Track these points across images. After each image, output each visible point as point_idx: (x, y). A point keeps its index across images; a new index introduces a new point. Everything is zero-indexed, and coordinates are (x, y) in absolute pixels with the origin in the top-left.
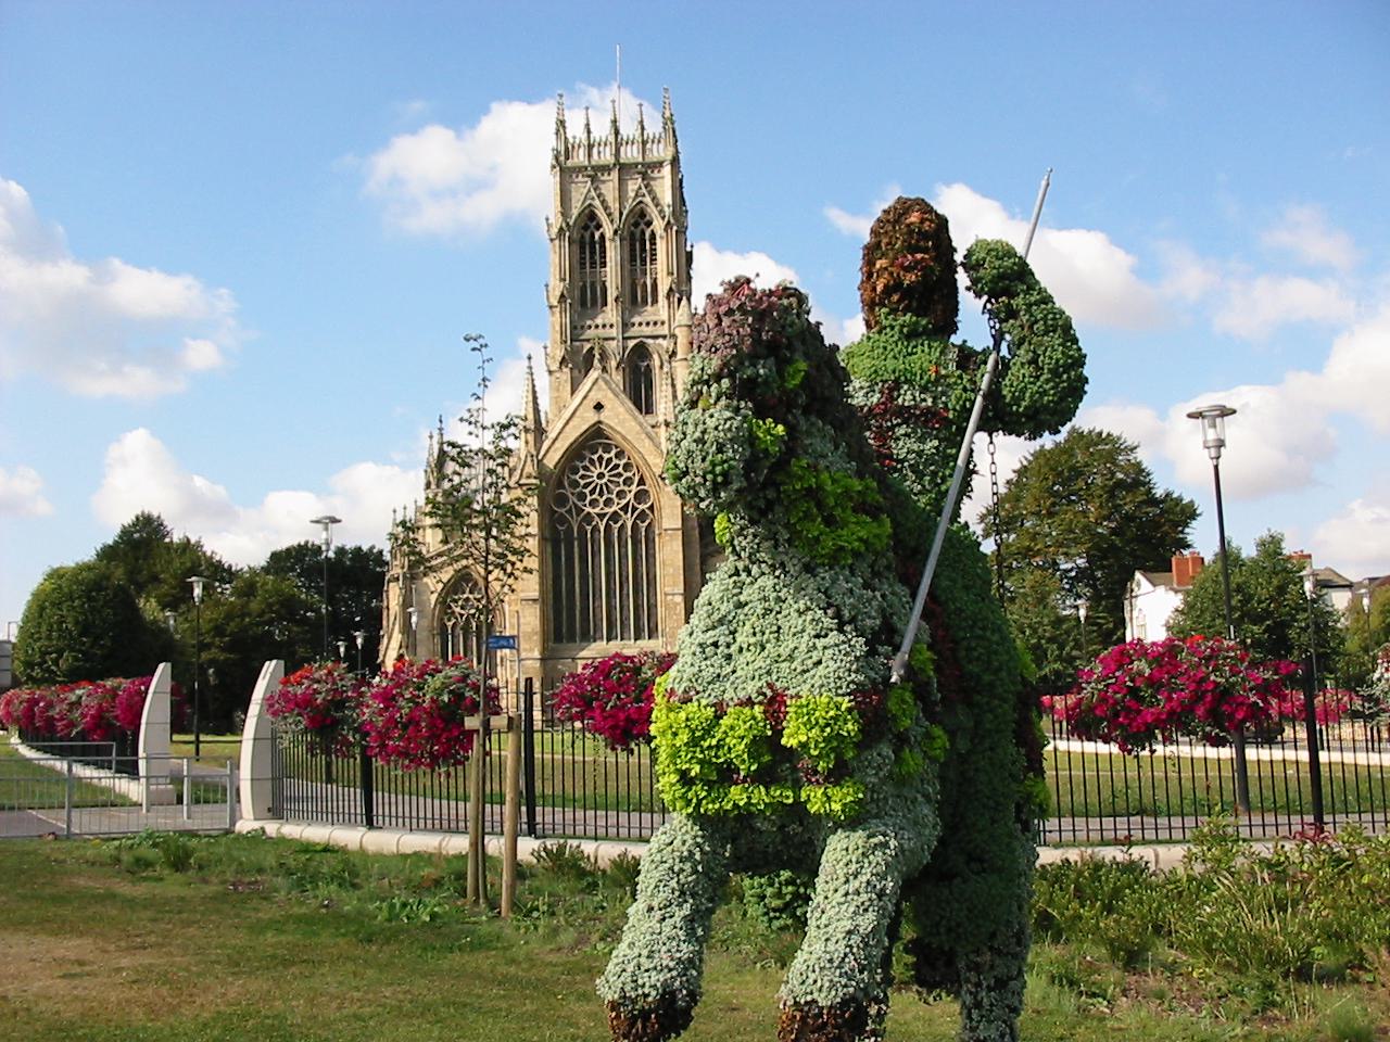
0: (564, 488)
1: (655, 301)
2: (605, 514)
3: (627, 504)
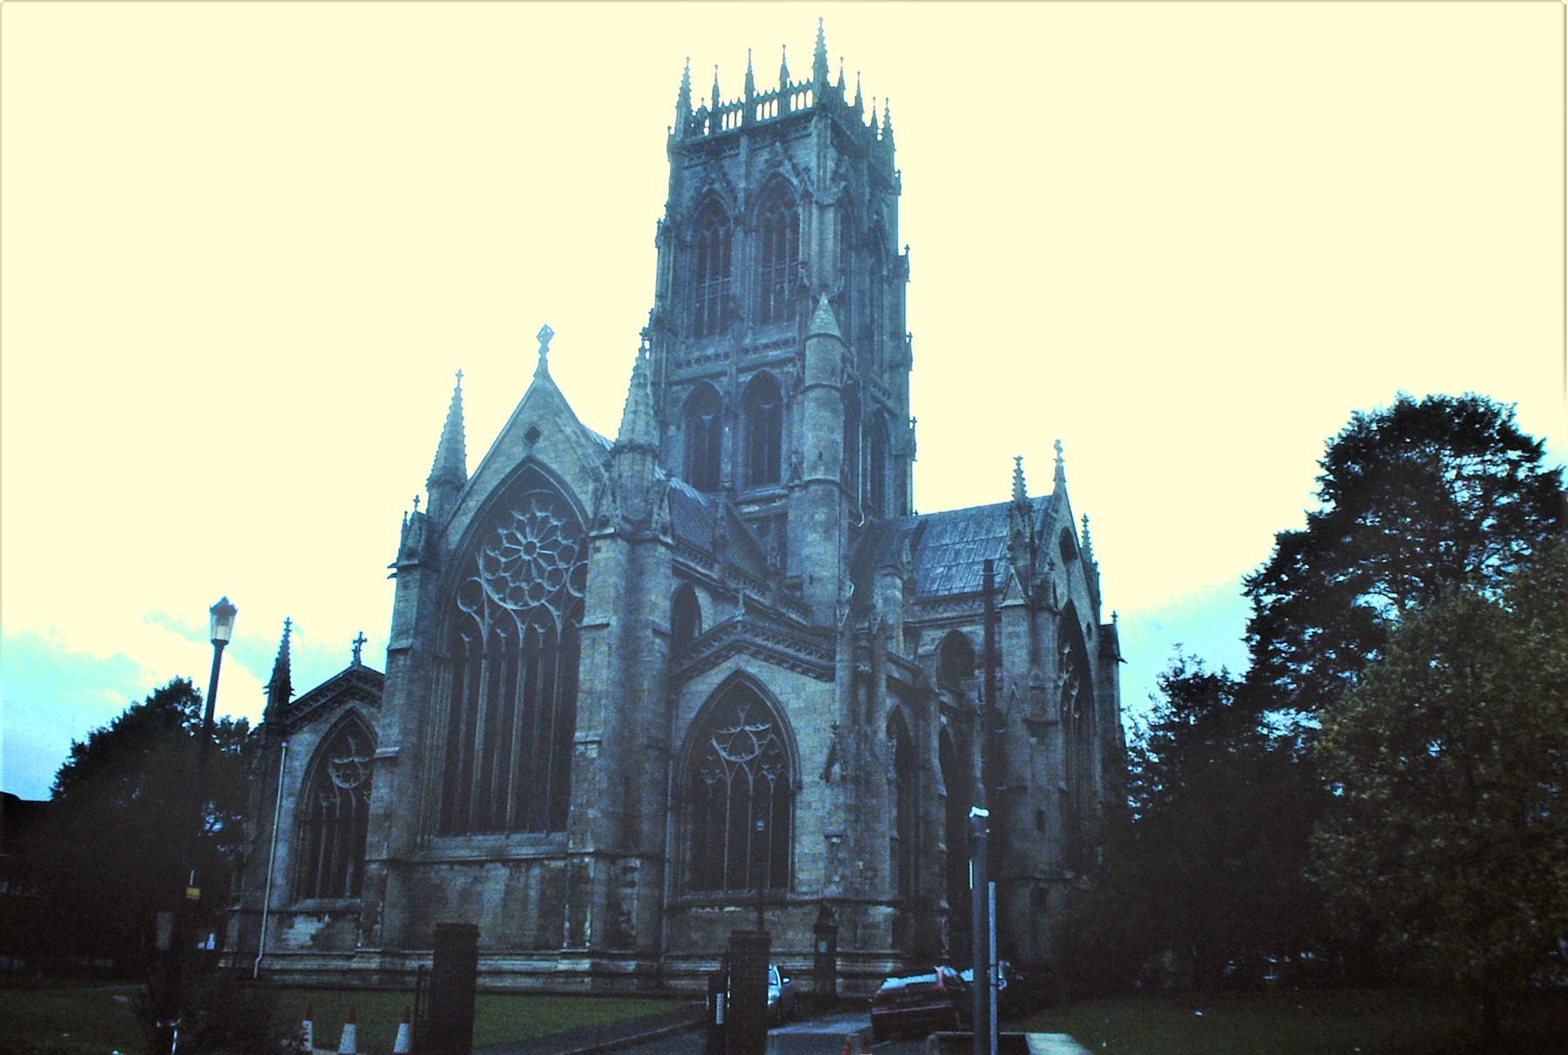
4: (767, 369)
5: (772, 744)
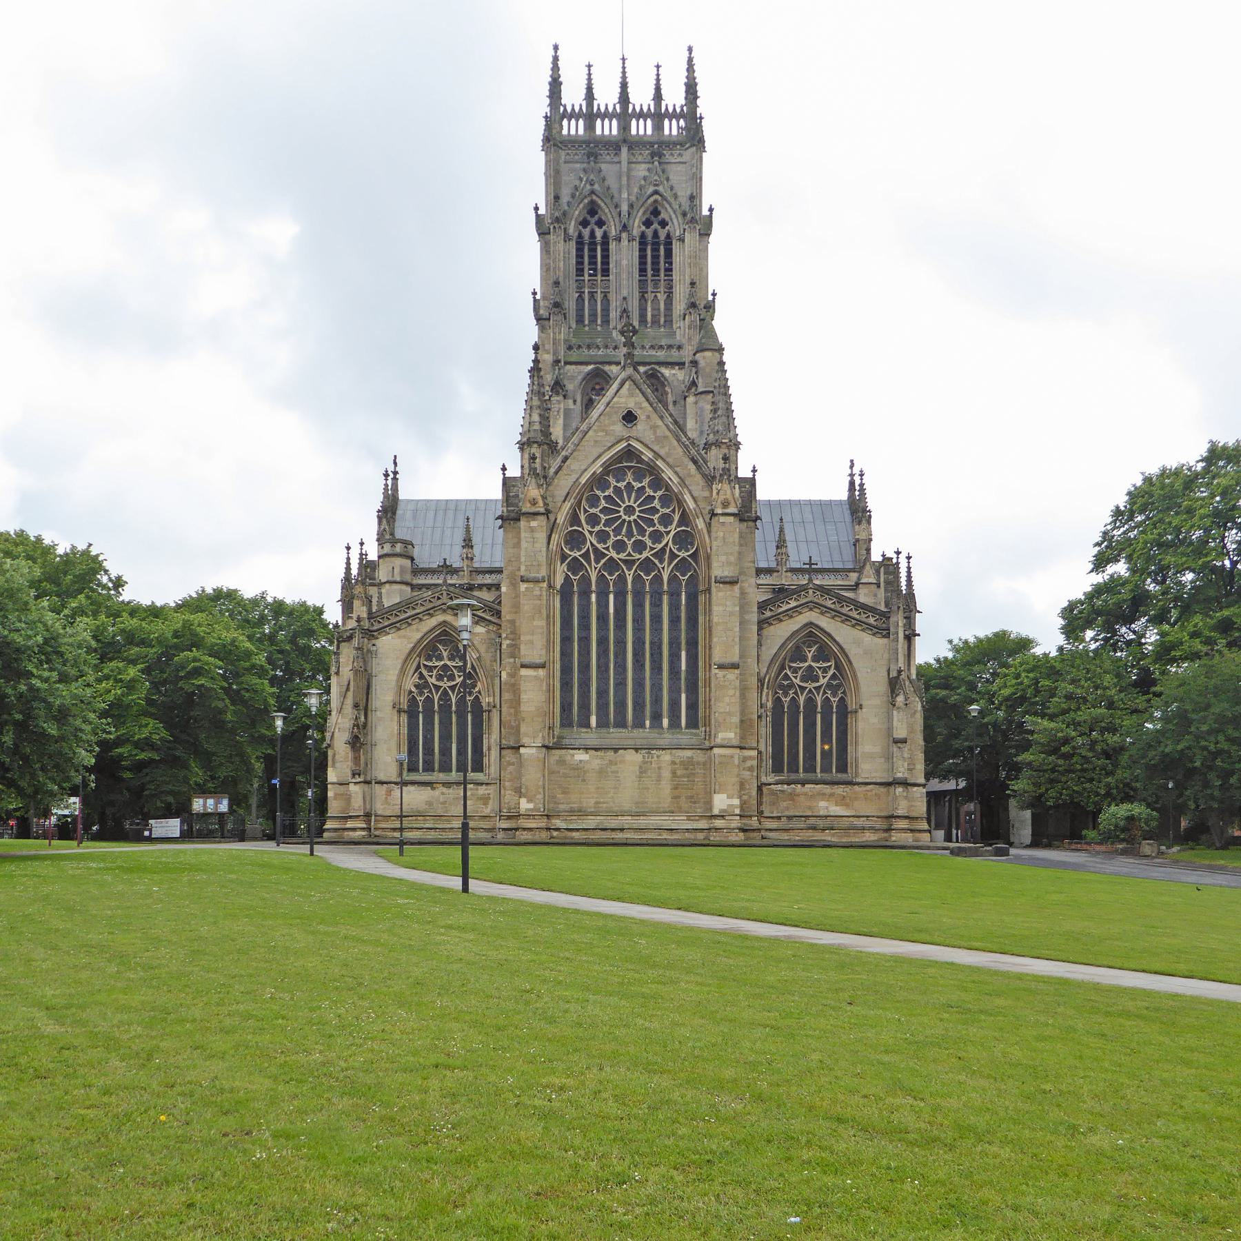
0: (580, 525)
1: (669, 321)
2: (634, 562)
3: (663, 550)
4: (657, 367)
5: (834, 677)
